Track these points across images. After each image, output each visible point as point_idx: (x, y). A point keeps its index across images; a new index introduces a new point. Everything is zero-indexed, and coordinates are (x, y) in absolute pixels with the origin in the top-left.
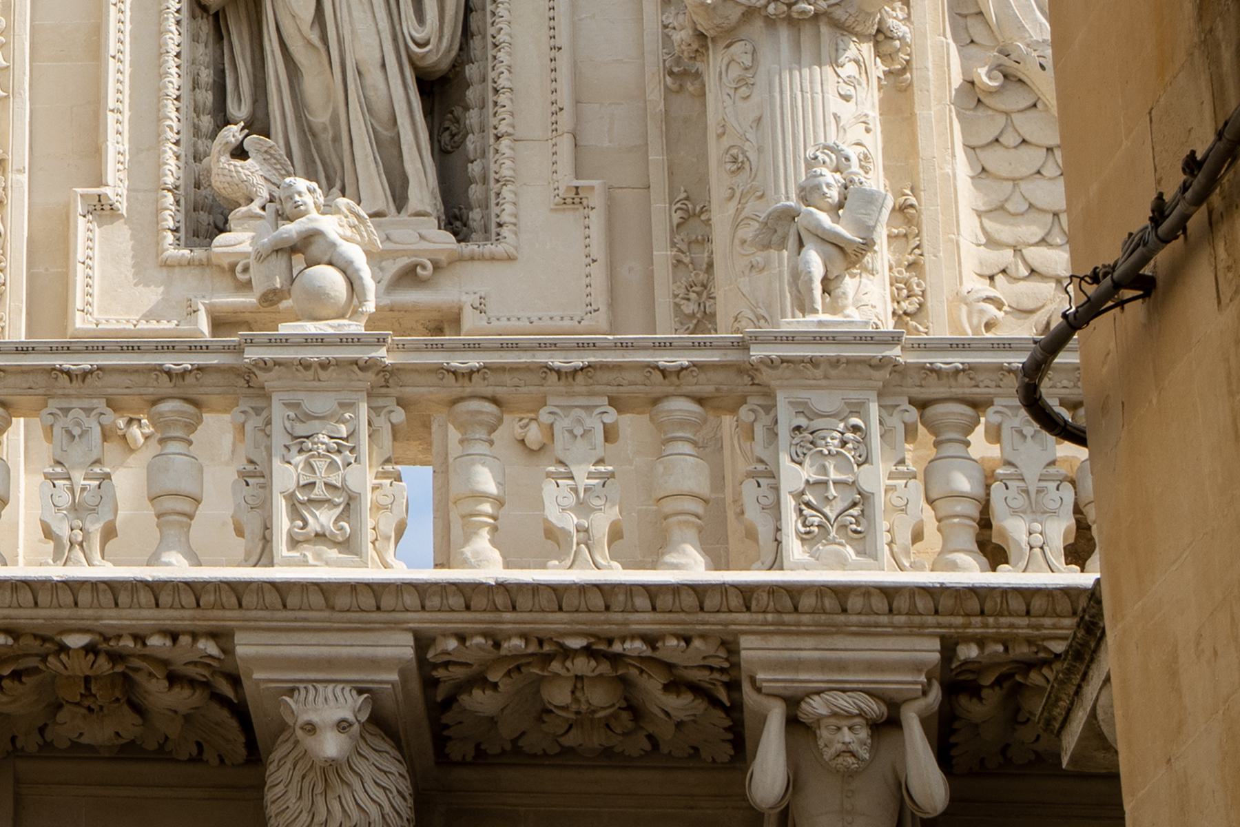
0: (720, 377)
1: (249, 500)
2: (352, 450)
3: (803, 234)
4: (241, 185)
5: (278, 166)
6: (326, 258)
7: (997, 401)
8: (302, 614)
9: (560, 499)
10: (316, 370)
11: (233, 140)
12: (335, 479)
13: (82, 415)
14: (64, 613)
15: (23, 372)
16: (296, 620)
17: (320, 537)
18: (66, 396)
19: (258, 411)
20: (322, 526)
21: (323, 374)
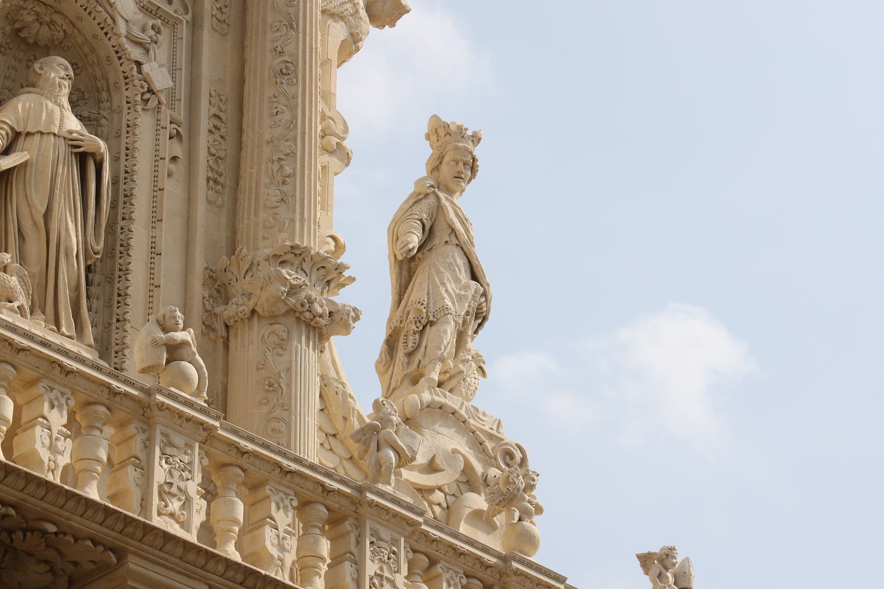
0: (344, 501)
1: (136, 479)
2: (190, 472)
3: (382, 442)
4: (9, 290)
5: (25, 288)
6: (189, 360)
7: (442, 562)
8: (167, 556)
9: (272, 538)
10: (182, 421)
11: (6, 262)
12: (182, 484)
13: (59, 395)
14: (54, 509)
15: (38, 357)
16: (162, 558)
17: (172, 515)
18: (53, 380)
19: (144, 431)
20: (174, 509)
21: (185, 424)
